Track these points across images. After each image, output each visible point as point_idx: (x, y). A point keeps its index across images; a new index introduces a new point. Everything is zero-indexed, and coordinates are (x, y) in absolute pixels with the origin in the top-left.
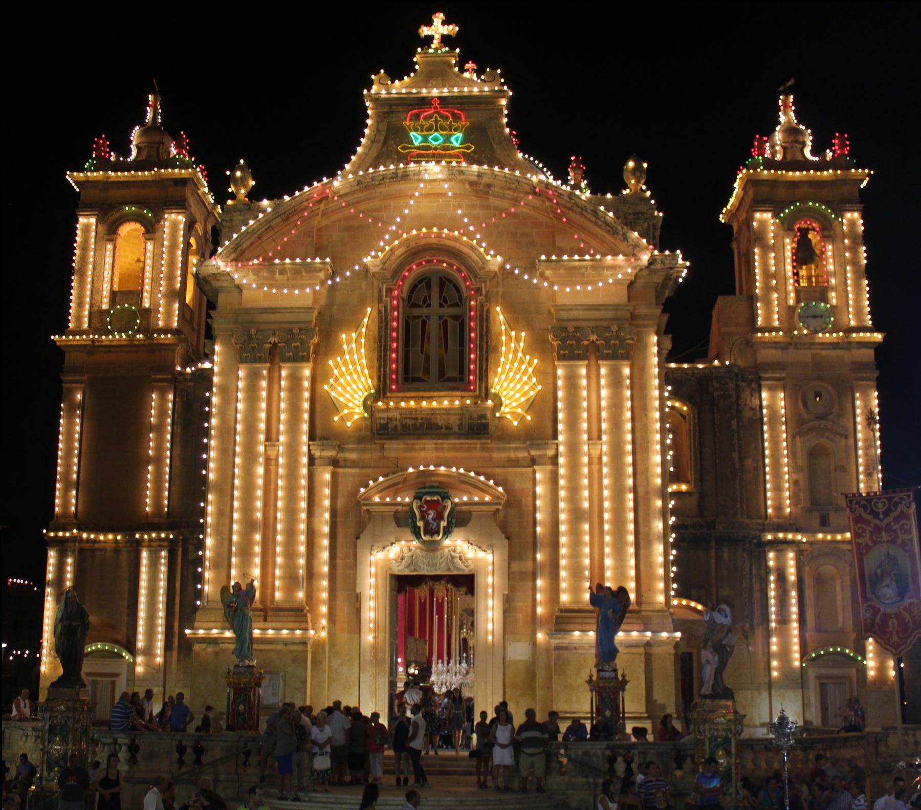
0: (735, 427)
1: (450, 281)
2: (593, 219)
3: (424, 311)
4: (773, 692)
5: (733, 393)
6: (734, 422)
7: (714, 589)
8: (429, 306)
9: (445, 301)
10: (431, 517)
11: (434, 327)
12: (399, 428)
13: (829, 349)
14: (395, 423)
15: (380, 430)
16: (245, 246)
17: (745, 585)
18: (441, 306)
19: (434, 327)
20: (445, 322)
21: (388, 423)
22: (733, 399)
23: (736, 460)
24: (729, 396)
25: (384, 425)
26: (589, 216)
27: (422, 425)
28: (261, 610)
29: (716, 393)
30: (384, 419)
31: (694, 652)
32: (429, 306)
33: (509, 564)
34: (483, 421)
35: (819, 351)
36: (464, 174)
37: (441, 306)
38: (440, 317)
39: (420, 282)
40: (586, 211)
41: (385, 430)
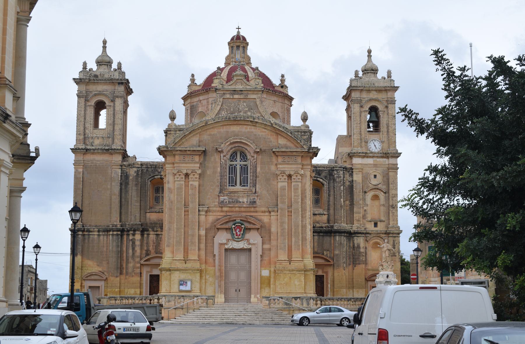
0: (342, 189)
1: (244, 153)
2: (290, 135)
3: (235, 163)
4: (354, 290)
5: (342, 176)
6: (342, 187)
7: (333, 251)
8: (236, 161)
9: (242, 160)
10: (238, 231)
11: (238, 167)
12: (227, 202)
13: (380, 158)
16: (177, 141)
17: (344, 250)
18: (240, 161)
19: (238, 167)
20: (242, 167)
22: (342, 178)
23: (342, 202)
24: (340, 177)
26: (289, 134)
27: (235, 201)
28: (184, 260)
29: (335, 176)
31: (325, 275)
32: (236, 161)
33: (262, 245)
35: (376, 159)
37: (240, 161)
38: (240, 165)
39: (233, 153)
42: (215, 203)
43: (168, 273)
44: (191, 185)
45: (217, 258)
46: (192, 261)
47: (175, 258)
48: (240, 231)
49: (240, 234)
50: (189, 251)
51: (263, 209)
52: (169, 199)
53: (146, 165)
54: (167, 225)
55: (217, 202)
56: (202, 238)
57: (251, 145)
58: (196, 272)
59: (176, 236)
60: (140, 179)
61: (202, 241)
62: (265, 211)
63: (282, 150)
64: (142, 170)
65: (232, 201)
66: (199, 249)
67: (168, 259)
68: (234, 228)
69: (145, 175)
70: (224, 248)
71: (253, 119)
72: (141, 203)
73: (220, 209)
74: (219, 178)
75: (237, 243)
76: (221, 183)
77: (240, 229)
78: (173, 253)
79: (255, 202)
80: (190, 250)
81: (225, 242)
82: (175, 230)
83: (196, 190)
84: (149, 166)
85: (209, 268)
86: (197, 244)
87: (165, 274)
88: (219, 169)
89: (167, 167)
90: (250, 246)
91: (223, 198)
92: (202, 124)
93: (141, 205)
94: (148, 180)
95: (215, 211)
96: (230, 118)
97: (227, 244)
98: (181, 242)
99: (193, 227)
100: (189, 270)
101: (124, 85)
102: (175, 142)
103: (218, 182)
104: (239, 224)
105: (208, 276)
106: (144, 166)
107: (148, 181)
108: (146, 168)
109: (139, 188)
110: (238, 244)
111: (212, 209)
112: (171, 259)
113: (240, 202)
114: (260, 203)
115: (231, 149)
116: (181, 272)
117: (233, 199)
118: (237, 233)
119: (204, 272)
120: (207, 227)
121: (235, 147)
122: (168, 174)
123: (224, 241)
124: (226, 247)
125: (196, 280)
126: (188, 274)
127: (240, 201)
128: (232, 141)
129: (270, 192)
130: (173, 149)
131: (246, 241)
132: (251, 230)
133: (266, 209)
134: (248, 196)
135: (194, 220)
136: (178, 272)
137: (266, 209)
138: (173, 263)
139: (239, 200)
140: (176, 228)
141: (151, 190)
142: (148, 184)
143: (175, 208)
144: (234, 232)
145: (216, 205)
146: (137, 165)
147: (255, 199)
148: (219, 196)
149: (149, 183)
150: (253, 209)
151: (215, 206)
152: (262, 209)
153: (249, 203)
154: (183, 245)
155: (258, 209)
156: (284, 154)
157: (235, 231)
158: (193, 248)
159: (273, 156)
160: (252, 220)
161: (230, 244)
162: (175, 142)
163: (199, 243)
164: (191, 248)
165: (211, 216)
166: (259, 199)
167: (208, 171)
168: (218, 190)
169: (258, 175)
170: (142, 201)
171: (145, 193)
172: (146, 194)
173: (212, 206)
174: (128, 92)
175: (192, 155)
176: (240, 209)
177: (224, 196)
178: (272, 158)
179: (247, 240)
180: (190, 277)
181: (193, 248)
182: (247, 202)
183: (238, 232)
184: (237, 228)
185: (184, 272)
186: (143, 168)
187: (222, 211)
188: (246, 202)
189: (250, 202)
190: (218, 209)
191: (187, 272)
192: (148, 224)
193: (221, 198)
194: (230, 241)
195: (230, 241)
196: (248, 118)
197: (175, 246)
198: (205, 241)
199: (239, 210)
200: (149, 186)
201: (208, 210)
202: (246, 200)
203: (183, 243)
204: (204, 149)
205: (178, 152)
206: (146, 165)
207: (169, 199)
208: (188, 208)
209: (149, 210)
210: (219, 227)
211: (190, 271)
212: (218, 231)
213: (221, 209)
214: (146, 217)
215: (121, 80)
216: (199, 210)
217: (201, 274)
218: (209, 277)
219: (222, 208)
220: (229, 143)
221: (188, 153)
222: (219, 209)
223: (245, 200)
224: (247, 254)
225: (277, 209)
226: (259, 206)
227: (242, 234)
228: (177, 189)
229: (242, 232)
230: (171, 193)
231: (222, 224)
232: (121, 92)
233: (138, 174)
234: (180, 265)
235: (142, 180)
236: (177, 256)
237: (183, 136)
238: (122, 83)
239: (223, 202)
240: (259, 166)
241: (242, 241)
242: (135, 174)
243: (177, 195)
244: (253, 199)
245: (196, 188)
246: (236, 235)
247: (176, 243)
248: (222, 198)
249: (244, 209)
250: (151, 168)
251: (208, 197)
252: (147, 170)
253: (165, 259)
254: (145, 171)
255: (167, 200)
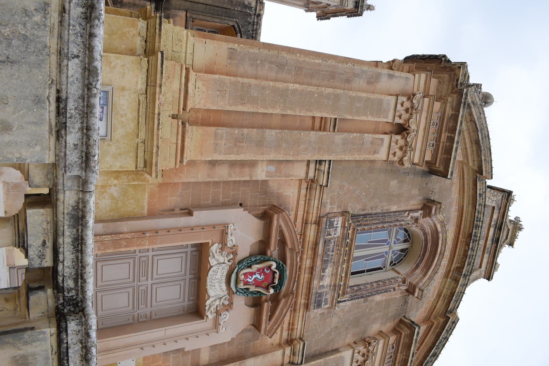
10: (258, 276)
14: (333, 234)
15: (330, 221)
16: (473, 110)
21: (333, 228)
25: (333, 224)
30: (337, 224)
34: (323, 303)
36: (468, 265)
40: (436, 349)
41: (329, 226)
42: (331, 204)
43: (139, 43)
44: (382, 140)
45: (183, 221)
46: (180, 142)
47: (192, 75)
48: (257, 283)
49: (246, 283)
50: (213, 129)
51: (298, 326)
52: (356, 75)
53: (257, 22)
54: (294, 57)
55: (332, 208)
56: (247, 170)
57: (427, 277)
58: (141, 154)
59: (264, 88)
60: (239, 9)
61: (238, 170)
62: (292, 329)
63: (413, 345)
64: (251, 15)
65: (329, 250)
66: (213, 163)
67: (189, 51)
68: (269, 267)
69: (244, 18)
70: (210, 242)
71: (464, 275)
72: (201, 5)
73: (313, 217)
74: (379, 211)
75: (224, 279)
76: (370, 214)
77: (263, 282)
78: (209, 71)
79: (319, 306)
80: (216, 135)
81: (229, 244)
82: (281, 85)
83: (369, 153)
84: (255, 27)
85: (147, 195)
86: (233, 157)
87: (134, 31)
88: (394, 208)
89: (420, 77)
90: (210, 316)
91: (339, 225)
92: (486, 171)
93: (199, 5)
94: (236, 22)
95: (308, 202)
96: (476, 228)
97: (221, 249)
98: (242, 104)
99: (284, 145)
100: (151, 132)
101: (354, 9)
102: (472, 105)
103: (372, 208)
104: (276, 281)
105: (115, 194)
106: (256, 18)
107: (235, 23)
108: (254, 22)
109: (225, 6)
110: (220, 282)
111: (317, 197)
112: (189, 62)
113: (323, 270)
114: (314, 318)
115: (425, 234)
116: (142, 98)
117: (333, 251)
118: (252, 274)
119: (134, 180)
120: (270, 183)
121: (426, 240)
122: (407, 78)
123: (231, 241)
124: (215, 248)
125: (108, 159)
126: (132, 126)
127: (327, 270)
128: (440, 235)
129: (333, 334)
130: (463, 101)
131: (227, 303)
132: (253, 309)
133: (297, 334)
134: (335, 286)
135: (302, 147)
136: (141, 85)
137: (298, 333)
138: (178, 68)
139: (329, 267)
140: (287, 90)
141: (219, 24)
142: (230, 21)
143: (339, 91)
144: (255, 267)
145: (325, 207)
146: (260, 8)
147: (326, 304)
148: (344, 213)
149: (231, 24)
150: (303, 301)
151: (321, 203)
152: (300, 323)
153: (319, 291)
154: (233, 108)
155: (301, 314)
156: (400, 347)
157: (259, 270)
158: (223, 142)
159: (395, 321)
160: (282, 310)
161: (221, 259)
162: (472, 105)
163: (233, 164)
164: (221, 139)
165: (296, 191)
166: (323, 313)
167: (396, 182)
168: (355, 208)
169: (370, 298)
170: (204, 6)
171: (216, 13)
172: (215, 16)
173: (325, 196)
174: (327, 14)
175: (438, 146)
176: (307, 271)
177: (343, 227)
178: (392, 320)
179: (231, 304)
180: (119, 133)
181: (223, 142)
182: (323, 286)
183: (254, 277)
184: (265, 274)
185: (142, 110)
186: (253, 17)
187: (305, 223)
188: (321, 284)
189: (320, 295)
190: (315, 212)
191: (142, 121)
192: (168, 12)
193: (340, 219)
194: (232, 256)
195: (232, 256)
196: (469, 264)
197: (233, 78)
198: (237, 179)
199: (304, 267)
200: (226, 22)
201: (314, 186)
202: (325, 284)
203: (241, 108)
204: (449, 177)
205: (449, 112)
206: (257, 22)
207: (356, 75)
208: (331, 129)
209: (191, 17)
210: (275, 222)
211: (142, 135)
212: (257, 216)
213: (314, 219)
214: (180, 10)
215: (362, 6)
216: (321, 161)
217: (127, 172)
218: (112, 198)
219: (315, 223)
220: (439, 229)
221: (444, 136)
222: (315, 215)
223: (327, 281)
224: (183, 304)
225: (299, 361)
226: (309, 316)
227: (248, 289)
228: (380, 100)
229: (252, 289)
230: (369, 83)
231: (281, 233)
232: (346, 4)
233: (246, 7)
234: (169, 95)
235: (236, 12)
236: (199, 84)
237: (478, 126)
238: (357, 7)
239: (331, 225)
240: (384, 298)
241: (226, 292)
242: (246, 3)
243: (368, 99)
244: (326, 300)
245: (375, 153)
246: (245, 274)
247: (243, 84)
248: (338, 222)
249: (306, 280)
250: (253, 31)
251: (346, 184)
252: (250, 23)
253: (191, 38)
254: (249, 19)
255: (355, 67)
